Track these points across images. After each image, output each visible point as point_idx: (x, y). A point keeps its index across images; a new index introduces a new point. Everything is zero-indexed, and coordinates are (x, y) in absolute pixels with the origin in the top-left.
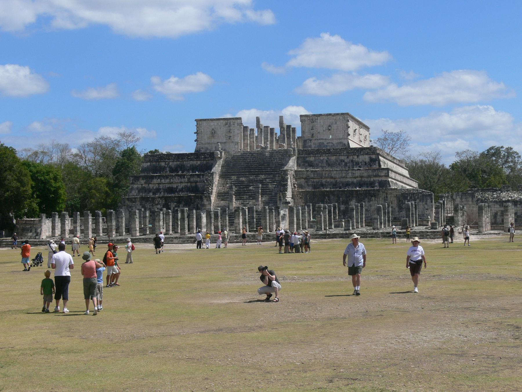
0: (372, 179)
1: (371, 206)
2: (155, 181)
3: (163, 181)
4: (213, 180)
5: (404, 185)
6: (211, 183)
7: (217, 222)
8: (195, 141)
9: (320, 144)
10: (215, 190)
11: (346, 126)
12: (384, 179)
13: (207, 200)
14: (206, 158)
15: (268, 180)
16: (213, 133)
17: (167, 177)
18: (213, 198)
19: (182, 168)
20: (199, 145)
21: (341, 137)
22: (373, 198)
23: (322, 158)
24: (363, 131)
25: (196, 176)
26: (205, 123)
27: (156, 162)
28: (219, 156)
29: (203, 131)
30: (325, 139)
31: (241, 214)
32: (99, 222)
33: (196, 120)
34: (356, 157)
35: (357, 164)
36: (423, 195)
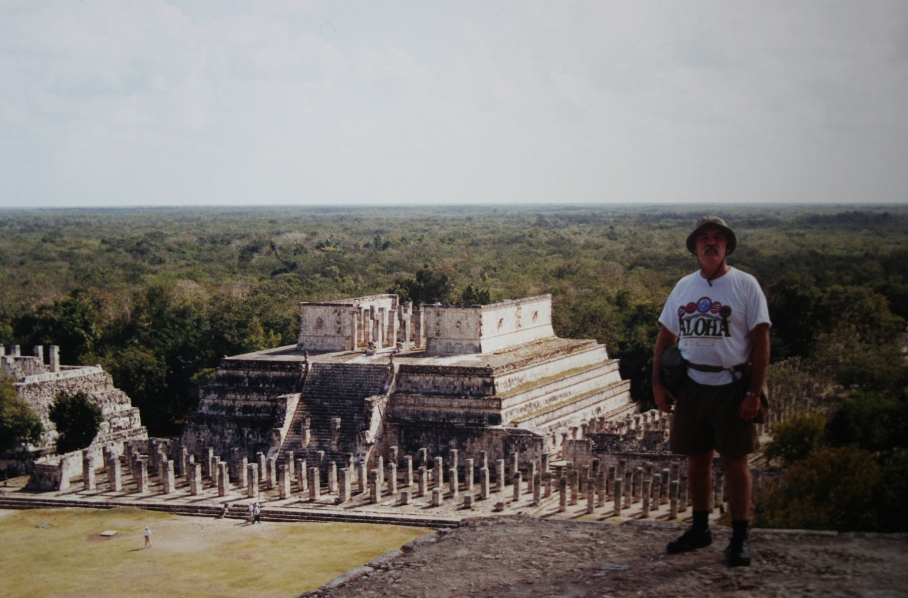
12: (495, 411)
22: (476, 439)
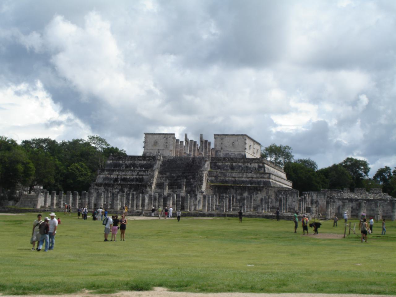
0: (259, 180)
1: (257, 197)
2: (115, 173)
3: (120, 173)
4: (154, 174)
5: (281, 184)
6: (153, 177)
7: (155, 203)
8: (143, 147)
9: (227, 154)
10: (155, 181)
11: (244, 143)
12: (267, 180)
13: (150, 188)
14: (150, 159)
15: (190, 176)
16: (156, 143)
17: (123, 171)
18: (153, 186)
19: (134, 165)
20: (145, 151)
21: (241, 150)
22: (259, 192)
23: (227, 164)
24: (256, 146)
25: (143, 172)
26: (150, 136)
27: (116, 160)
28: (159, 159)
29: (149, 141)
30: (230, 151)
31: (171, 198)
32: (76, 199)
33: (144, 133)
35: (250, 168)
36: (292, 192)
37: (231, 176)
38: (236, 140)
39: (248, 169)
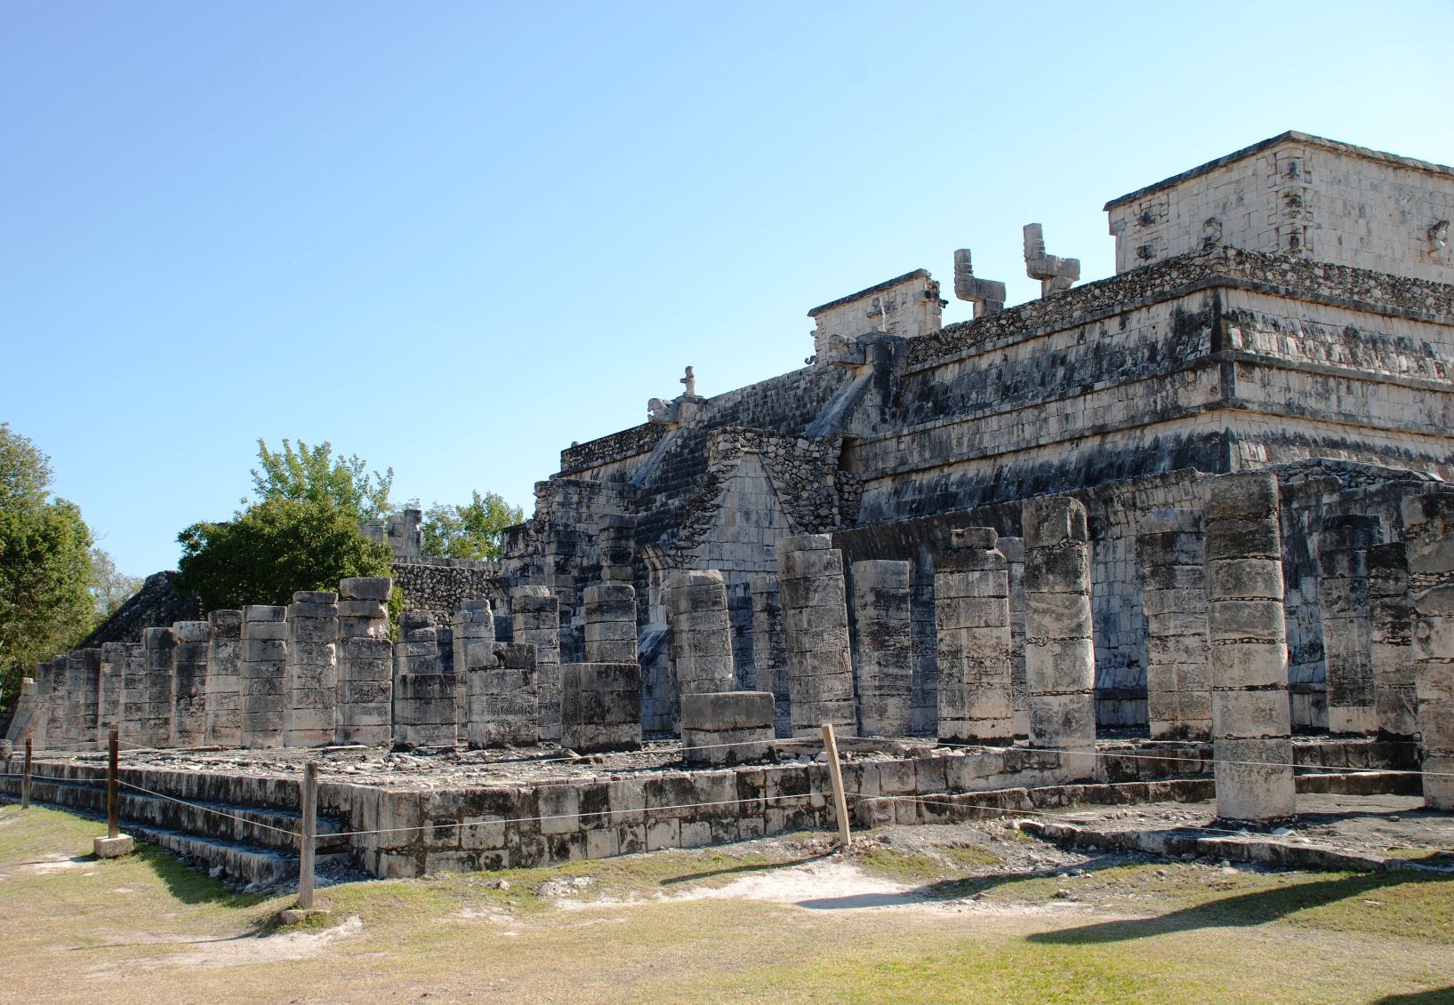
12: (1206, 424)
34: (1113, 325)
37: (971, 447)
38: (1233, 198)
39: (1105, 363)
